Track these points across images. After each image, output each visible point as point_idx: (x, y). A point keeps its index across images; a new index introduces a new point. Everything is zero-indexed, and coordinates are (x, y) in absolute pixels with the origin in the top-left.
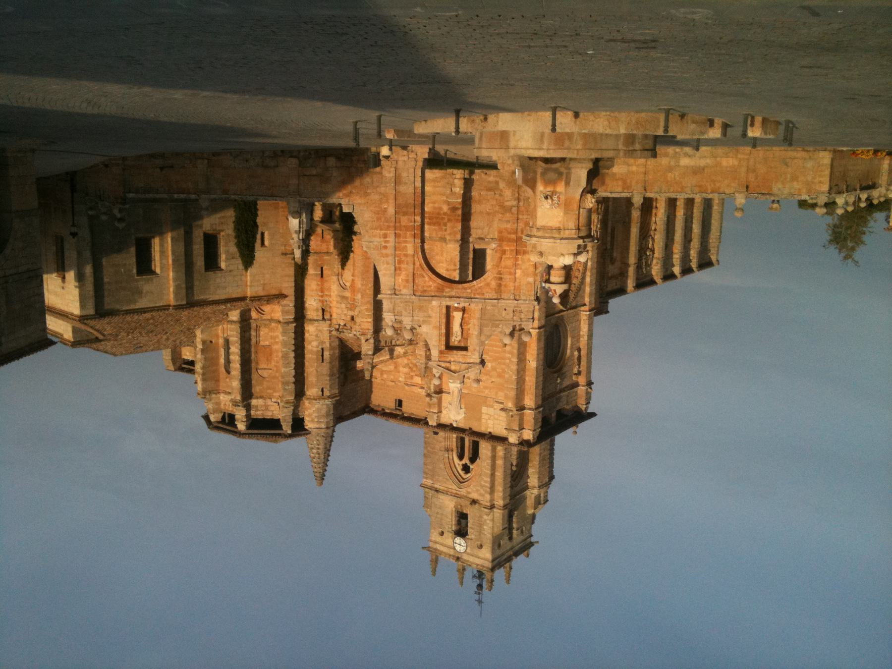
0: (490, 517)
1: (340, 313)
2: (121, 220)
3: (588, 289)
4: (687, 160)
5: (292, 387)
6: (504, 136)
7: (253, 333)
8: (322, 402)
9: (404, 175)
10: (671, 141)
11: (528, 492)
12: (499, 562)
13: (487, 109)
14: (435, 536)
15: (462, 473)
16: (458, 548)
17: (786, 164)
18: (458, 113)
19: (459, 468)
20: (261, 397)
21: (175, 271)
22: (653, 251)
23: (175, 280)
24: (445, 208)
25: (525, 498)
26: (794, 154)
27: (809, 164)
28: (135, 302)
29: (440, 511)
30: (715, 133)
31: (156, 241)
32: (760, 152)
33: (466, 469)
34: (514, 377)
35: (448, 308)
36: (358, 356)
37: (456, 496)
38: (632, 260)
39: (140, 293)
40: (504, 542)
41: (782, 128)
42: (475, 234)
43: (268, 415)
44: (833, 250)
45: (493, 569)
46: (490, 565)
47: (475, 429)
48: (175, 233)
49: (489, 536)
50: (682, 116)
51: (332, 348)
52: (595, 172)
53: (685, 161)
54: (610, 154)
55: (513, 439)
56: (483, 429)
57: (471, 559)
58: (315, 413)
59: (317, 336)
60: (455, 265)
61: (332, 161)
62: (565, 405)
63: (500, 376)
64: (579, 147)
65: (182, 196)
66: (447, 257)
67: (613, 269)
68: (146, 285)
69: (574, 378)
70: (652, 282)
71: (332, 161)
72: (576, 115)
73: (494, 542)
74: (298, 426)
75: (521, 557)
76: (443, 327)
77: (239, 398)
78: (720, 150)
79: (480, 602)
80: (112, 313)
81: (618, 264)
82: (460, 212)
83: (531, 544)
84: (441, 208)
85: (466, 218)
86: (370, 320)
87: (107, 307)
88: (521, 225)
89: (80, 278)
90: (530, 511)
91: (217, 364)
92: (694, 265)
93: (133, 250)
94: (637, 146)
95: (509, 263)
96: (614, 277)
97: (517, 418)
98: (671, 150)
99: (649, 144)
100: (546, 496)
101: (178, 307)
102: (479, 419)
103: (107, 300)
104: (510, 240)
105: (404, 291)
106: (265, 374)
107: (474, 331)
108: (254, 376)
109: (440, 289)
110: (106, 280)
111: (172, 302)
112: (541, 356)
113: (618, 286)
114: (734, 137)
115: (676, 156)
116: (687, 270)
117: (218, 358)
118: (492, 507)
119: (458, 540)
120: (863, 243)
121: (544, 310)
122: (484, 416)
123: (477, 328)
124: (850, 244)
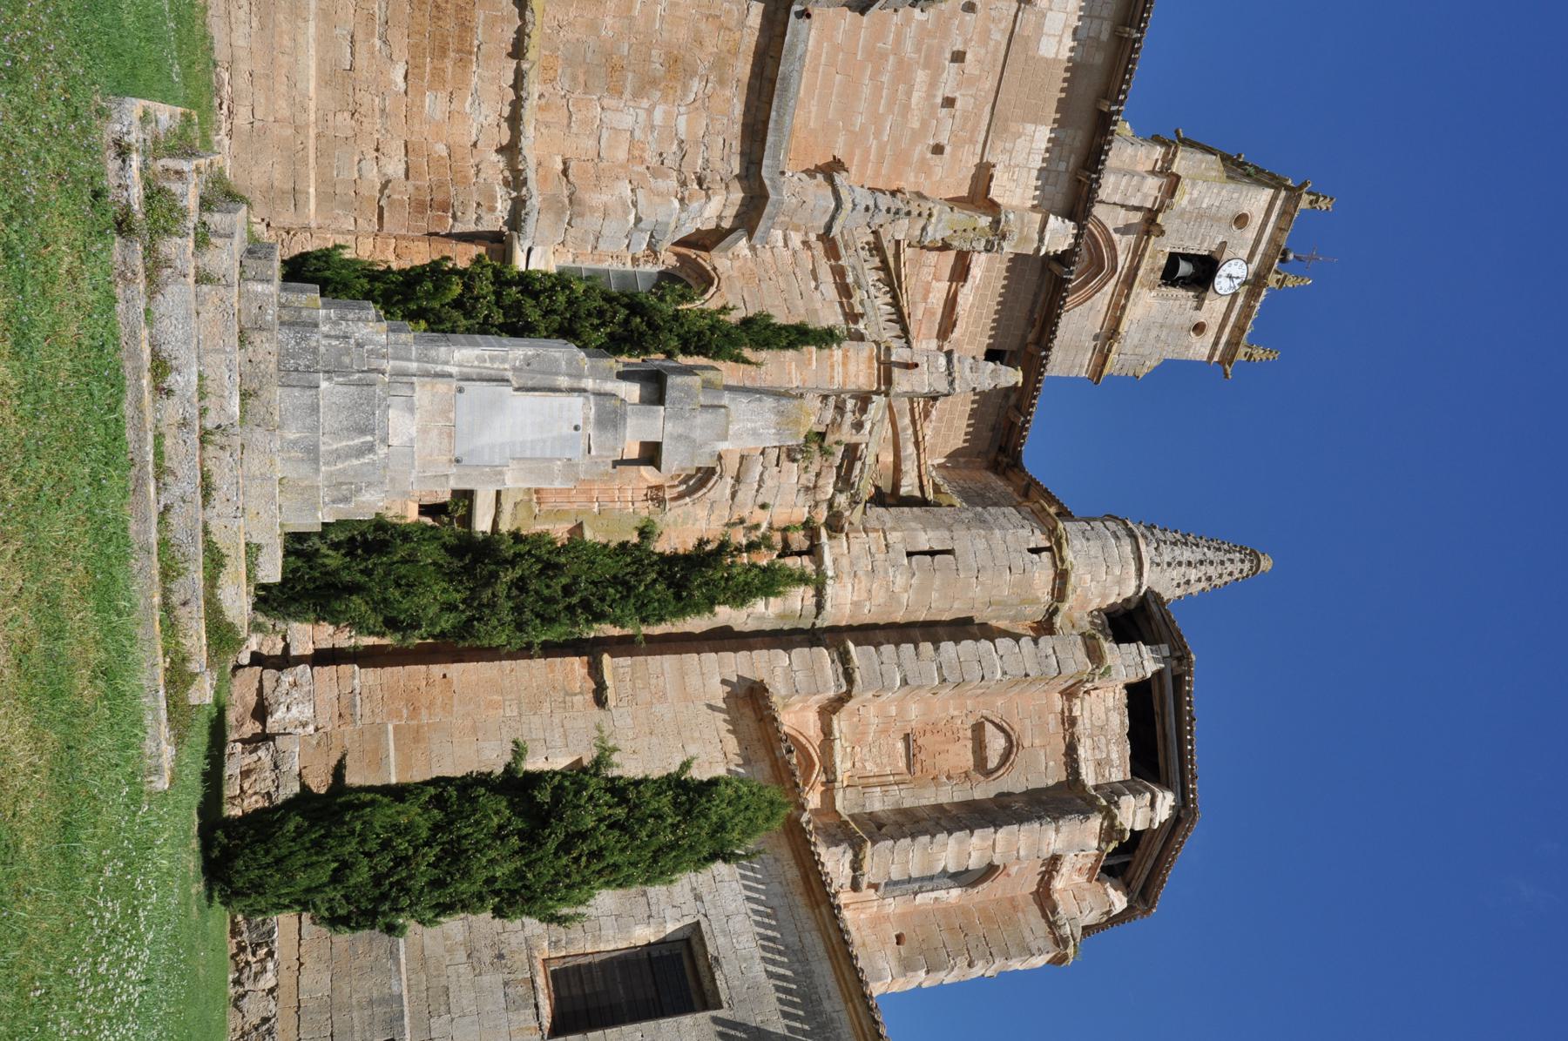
8: (1068, 554)
14: (1199, 349)
20: (1071, 750)
29: (1153, 334)
43: (1119, 722)
91: (964, 910)
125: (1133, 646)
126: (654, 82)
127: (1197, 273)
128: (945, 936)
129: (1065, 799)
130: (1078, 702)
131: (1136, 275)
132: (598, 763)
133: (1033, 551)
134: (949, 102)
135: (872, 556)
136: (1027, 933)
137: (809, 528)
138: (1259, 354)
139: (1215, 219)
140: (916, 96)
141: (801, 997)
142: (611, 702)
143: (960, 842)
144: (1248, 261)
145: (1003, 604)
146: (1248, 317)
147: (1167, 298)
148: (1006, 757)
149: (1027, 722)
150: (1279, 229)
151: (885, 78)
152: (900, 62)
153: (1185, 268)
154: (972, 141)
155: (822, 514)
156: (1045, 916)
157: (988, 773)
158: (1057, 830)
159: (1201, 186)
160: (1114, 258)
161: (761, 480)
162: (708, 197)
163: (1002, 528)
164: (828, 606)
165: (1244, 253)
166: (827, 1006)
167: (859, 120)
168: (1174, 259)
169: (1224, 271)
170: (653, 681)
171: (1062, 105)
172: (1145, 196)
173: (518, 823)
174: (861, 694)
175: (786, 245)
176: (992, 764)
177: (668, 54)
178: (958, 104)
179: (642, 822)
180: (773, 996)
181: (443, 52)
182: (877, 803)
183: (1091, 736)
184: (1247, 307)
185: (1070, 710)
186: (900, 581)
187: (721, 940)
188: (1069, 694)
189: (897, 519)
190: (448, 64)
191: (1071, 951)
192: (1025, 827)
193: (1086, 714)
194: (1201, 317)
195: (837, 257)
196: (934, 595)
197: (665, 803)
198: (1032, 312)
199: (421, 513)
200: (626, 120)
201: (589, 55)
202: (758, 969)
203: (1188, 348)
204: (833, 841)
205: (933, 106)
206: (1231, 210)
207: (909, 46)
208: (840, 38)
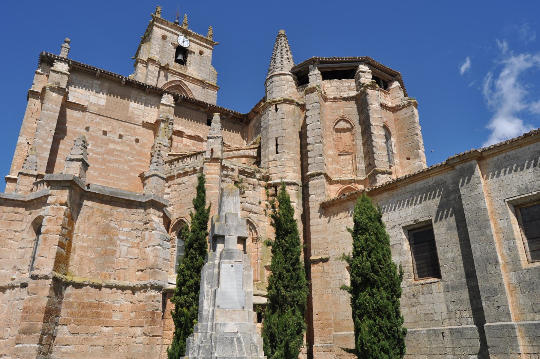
8: (278, 99)
14: (208, 53)
20: (345, 99)
21: (480, 211)
29: (202, 68)
43: (335, 83)
60: (45, 239)
91: (399, 137)
117: (399, 142)
125: (309, 77)
126: (111, 239)
127: (182, 53)
128: (407, 143)
129: (361, 101)
130: (328, 96)
131: (182, 74)
132: (348, 260)
133: (277, 111)
134: (121, 136)
135: (277, 166)
136: (406, 115)
137: (267, 187)
138: (210, 33)
139: (163, 46)
140: (118, 148)
141: (427, 192)
142: (327, 256)
143: (376, 137)
144: (178, 35)
145: (294, 121)
146: (197, 36)
147: (190, 64)
148: (347, 121)
149: (335, 114)
150: (167, 25)
151: (112, 158)
152: (106, 153)
153: (180, 57)
154: (134, 129)
155: (263, 183)
156: (401, 109)
157: (352, 127)
158: (372, 104)
159: (152, 51)
160: (176, 81)
161: (251, 203)
162: (152, 220)
163: (268, 121)
164: (294, 181)
165: (176, 37)
166: (431, 183)
167: (126, 168)
168: (177, 61)
169: (181, 44)
170: (320, 242)
171: (123, 97)
172: (155, 70)
173: (368, 289)
174: (325, 170)
175: (169, 194)
176: (349, 126)
177: (101, 234)
178: (121, 133)
179: (368, 246)
180: (428, 202)
181: (98, 313)
182: (362, 165)
183: (340, 92)
184: (194, 36)
185: (331, 99)
186: (286, 156)
187: (409, 219)
188: (326, 99)
189: (265, 157)
190: (103, 312)
191: (412, 101)
192: (371, 115)
193: (333, 94)
194: (197, 52)
195: (174, 176)
196: (291, 145)
197: (362, 238)
198: (194, 109)
199: (260, 322)
200: (124, 249)
201: (101, 262)
202: (418, 207)
203: (208, 57)
204: (375, 181)
205: (122, 142)
206: (160, 41)
207: (101, 150)
208: (97, 174)
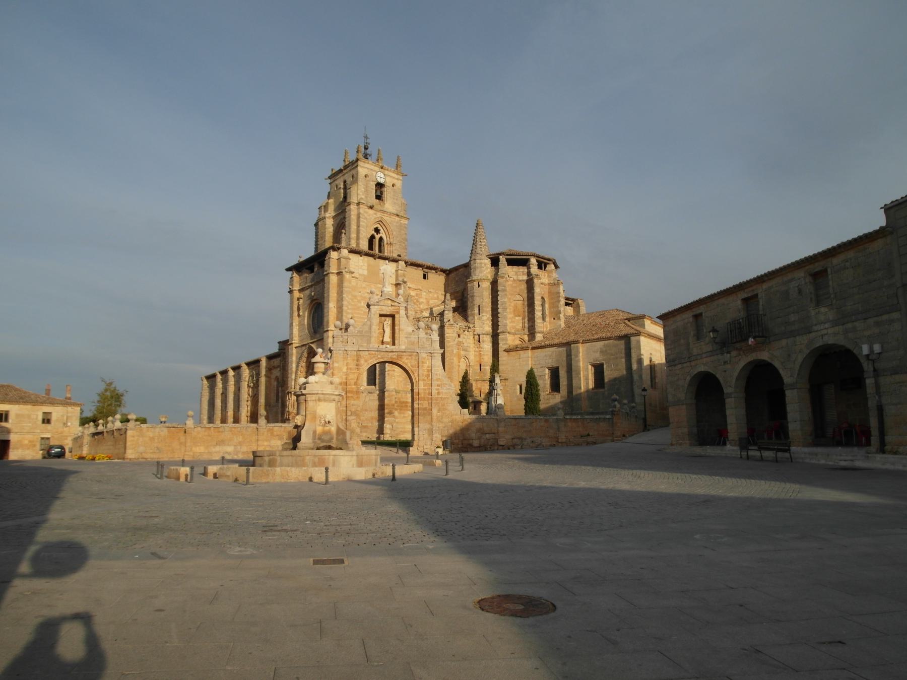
0: (360, 197)
1: (468, 339)
2: (615, 400)
3: (294, 358)
4: (228, 451)
5: (500, 288)
6: (360, 464)
7: (526, 325)
9: (426, 436)
10: (242, 463)
11: (333, 214)
12: (354, 164)
13: (374, 482)
14: (399, 184)
15: (380, 228)
16: (382, 175)
17: (158, 449)
18: (394, 478)
19: (382, 231)
22: (249, 386)
23: (578, 361)
24: (396, 413)
25: (335, 210)
26: (152, 456)
27: (141, 449)
28: (604, 346)
30: (212, 469)
31: (591, 385)
32: (178, 457)
33: (377, 231)
34: (344, 296)
35: (394, 344)
36: (455, 310)
37: (384, 212)
38: (263, 380)
39: (602, 352)
40: (349, 180)
41: (165, 474)
42: (375, 396)
43: (515, 268)
44: (120, 390)
45: (357, 160)
46: (359, 163)
47: (372, 259)
48: (579, 392)
49: (360, 183)
50: (236, 480)
51: (473, 315)
52: (296, 439)
53: (230, 449)
54: (285, 453)
55: (345, 252)
56: (366, 258)
57: (373, 167)
58: (483, 270)
59: (483, 323)
61: (476, 443)
62: (308, 276)
63: (355, 297)
64: (308, 458)
65: (574, 417)
66: (394, 379)
67: (277, 373)
68: (598, 357)
69: (302, 296)
70: (248, 364)
71: (476, 443)
72: (311, 479)
73: (357, 179)
74: (495, 262)
75: (337, 169)
76: (397, 331)
77: (535, 281)
78: (206, 457)
79: (366, 137)
80: (620, 338)
81: (273, 377)
82: (386, 411)
83: (330, 178)
84: (400, 413)
85: (382, 407)
86: (446, 335)
87: (623, 342)
88: (344, 403)
89: (640, 361)
90: (331, 201)
91: (550, 303)
92: (219, 377)
93: (606, 380)
94: (267, 459)
95: (351, 376)
96: (275, 367)
97: (342, 267)
98: (240, 457)
99: (258, 460)
100: (320, 212)
101: (577, 342)
102: (369, 265)
103: (623, 347)
104: (351, 392)
105: (425, 355)
106: (518, 297)
107: (375, 328)
108: (525, 295)
109: (400, 357)
110: (624, 360)
111: (580, 345)
112: (325, 311)
113: (272, 361)
114: (199, 468)
115: (237, 453)
116: (224, 373)
117: (550, 308)
118: (358, 204)
119: (382, 181)
120: (99, 395)
121: (325, 343)
122: (365, 268)
123: (373, 330)
124: (108, 394)
